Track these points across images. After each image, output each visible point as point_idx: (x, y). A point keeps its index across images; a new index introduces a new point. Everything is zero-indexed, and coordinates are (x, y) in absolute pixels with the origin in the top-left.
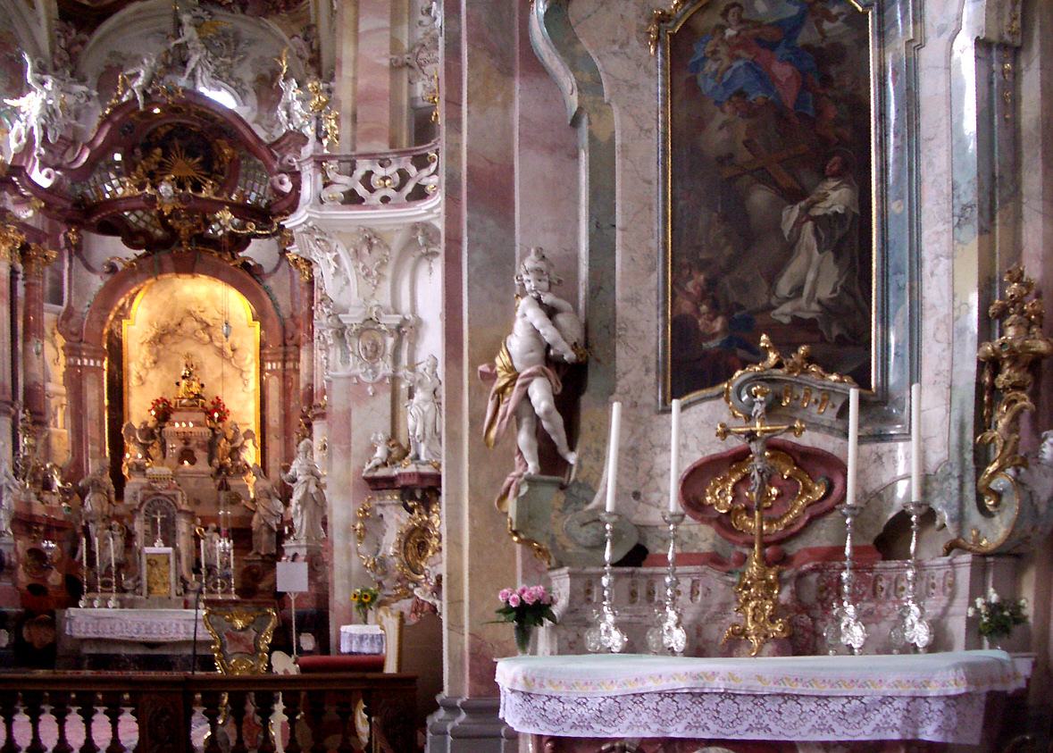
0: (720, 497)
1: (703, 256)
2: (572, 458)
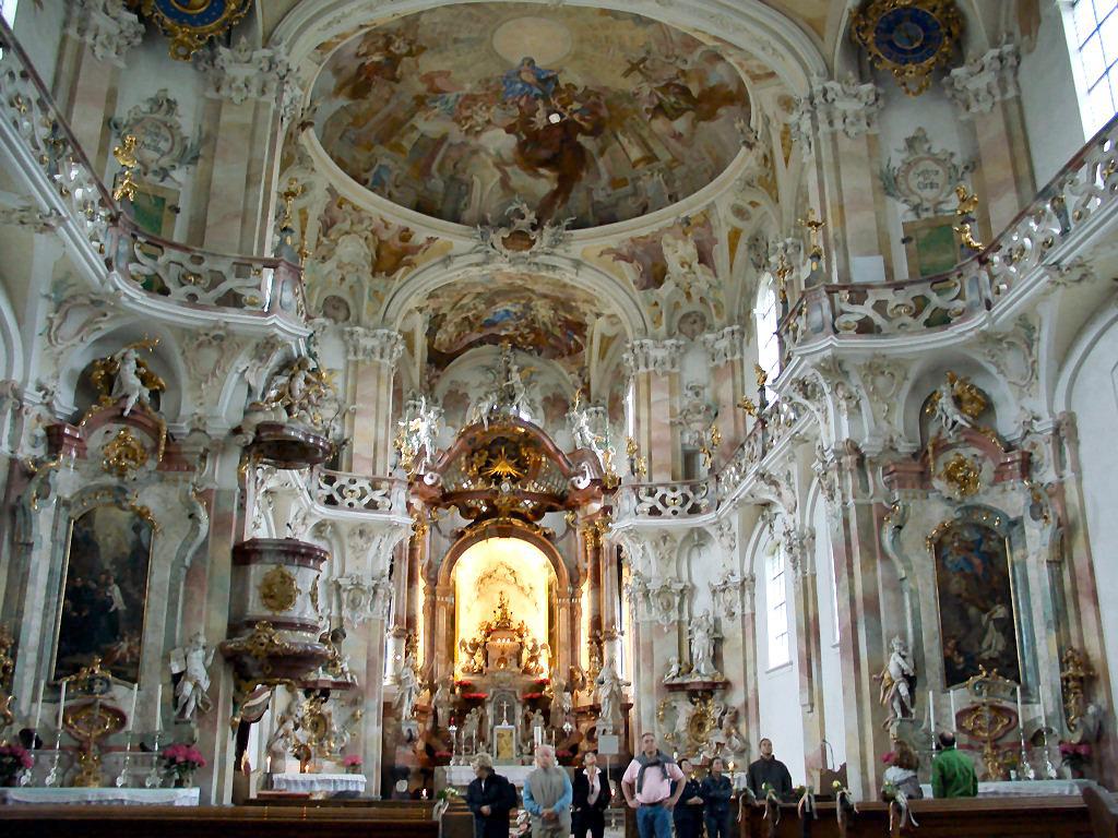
0: (968, 723)
1: (953, 633)
2: (913, 711)
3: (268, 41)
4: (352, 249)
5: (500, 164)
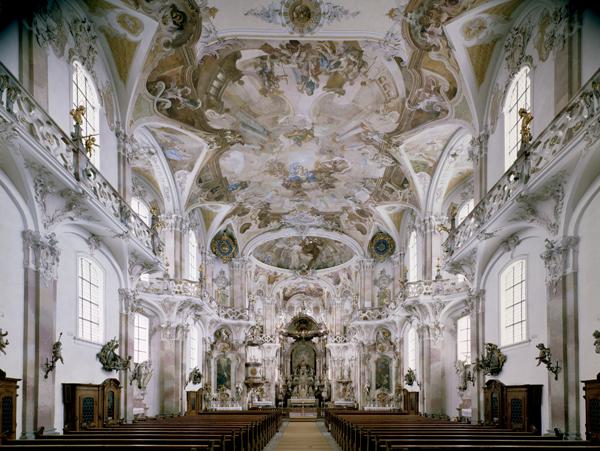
3: (242, 255)
4: (263, 278)
5: (298, 253)
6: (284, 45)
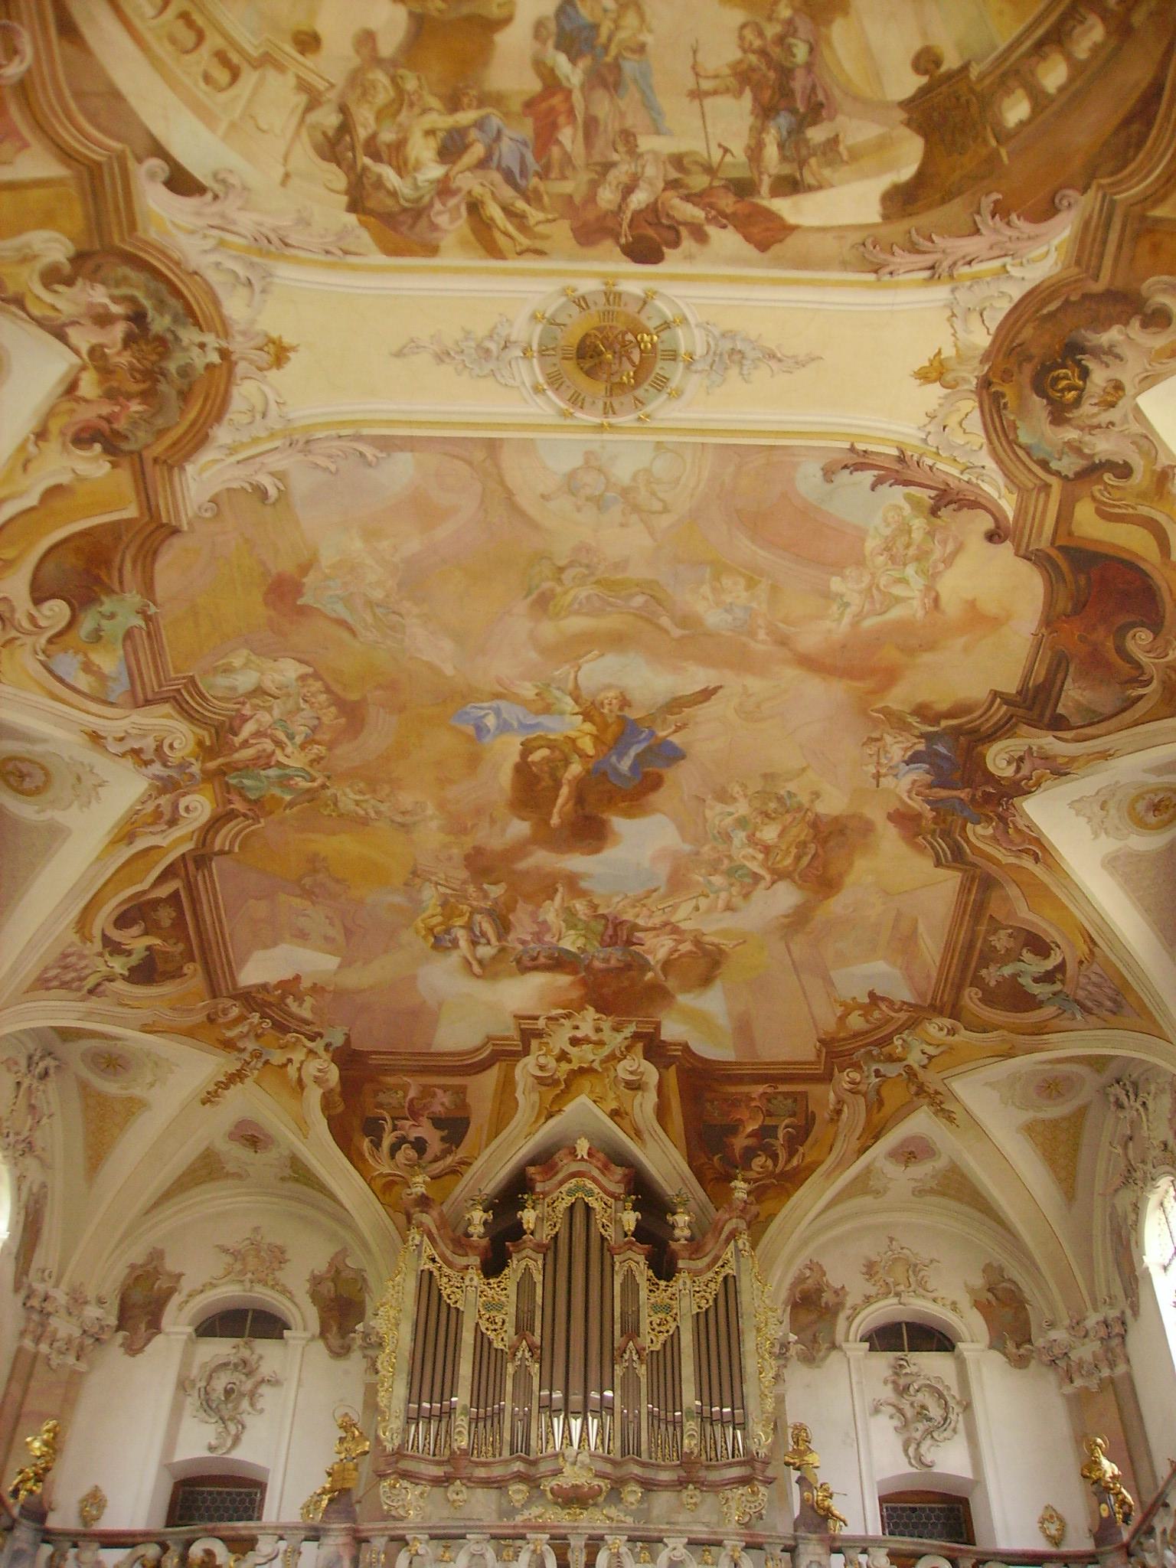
6: (688, 243)
